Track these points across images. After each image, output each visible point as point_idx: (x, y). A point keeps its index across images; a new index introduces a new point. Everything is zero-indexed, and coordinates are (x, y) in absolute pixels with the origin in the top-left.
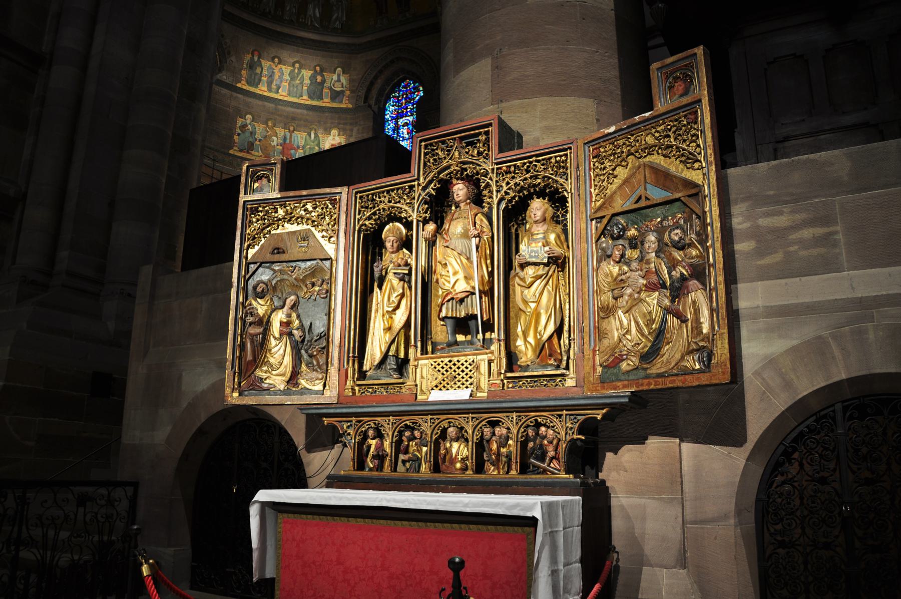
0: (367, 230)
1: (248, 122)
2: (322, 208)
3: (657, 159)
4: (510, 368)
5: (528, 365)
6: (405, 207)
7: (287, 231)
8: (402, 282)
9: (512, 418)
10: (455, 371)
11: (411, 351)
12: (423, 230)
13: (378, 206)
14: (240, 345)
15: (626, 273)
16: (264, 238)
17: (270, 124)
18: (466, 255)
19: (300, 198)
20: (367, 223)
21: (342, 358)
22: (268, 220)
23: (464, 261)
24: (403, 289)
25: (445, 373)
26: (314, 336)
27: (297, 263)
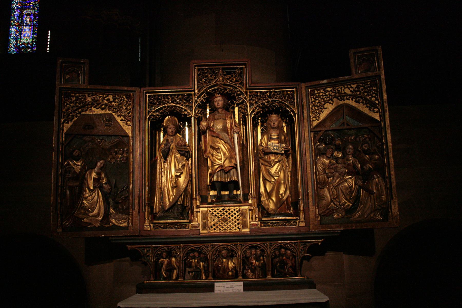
3: (352, 103)
7: (94, 113)
9: (267, 244)
15: (335, 164)
25: (220, 216)
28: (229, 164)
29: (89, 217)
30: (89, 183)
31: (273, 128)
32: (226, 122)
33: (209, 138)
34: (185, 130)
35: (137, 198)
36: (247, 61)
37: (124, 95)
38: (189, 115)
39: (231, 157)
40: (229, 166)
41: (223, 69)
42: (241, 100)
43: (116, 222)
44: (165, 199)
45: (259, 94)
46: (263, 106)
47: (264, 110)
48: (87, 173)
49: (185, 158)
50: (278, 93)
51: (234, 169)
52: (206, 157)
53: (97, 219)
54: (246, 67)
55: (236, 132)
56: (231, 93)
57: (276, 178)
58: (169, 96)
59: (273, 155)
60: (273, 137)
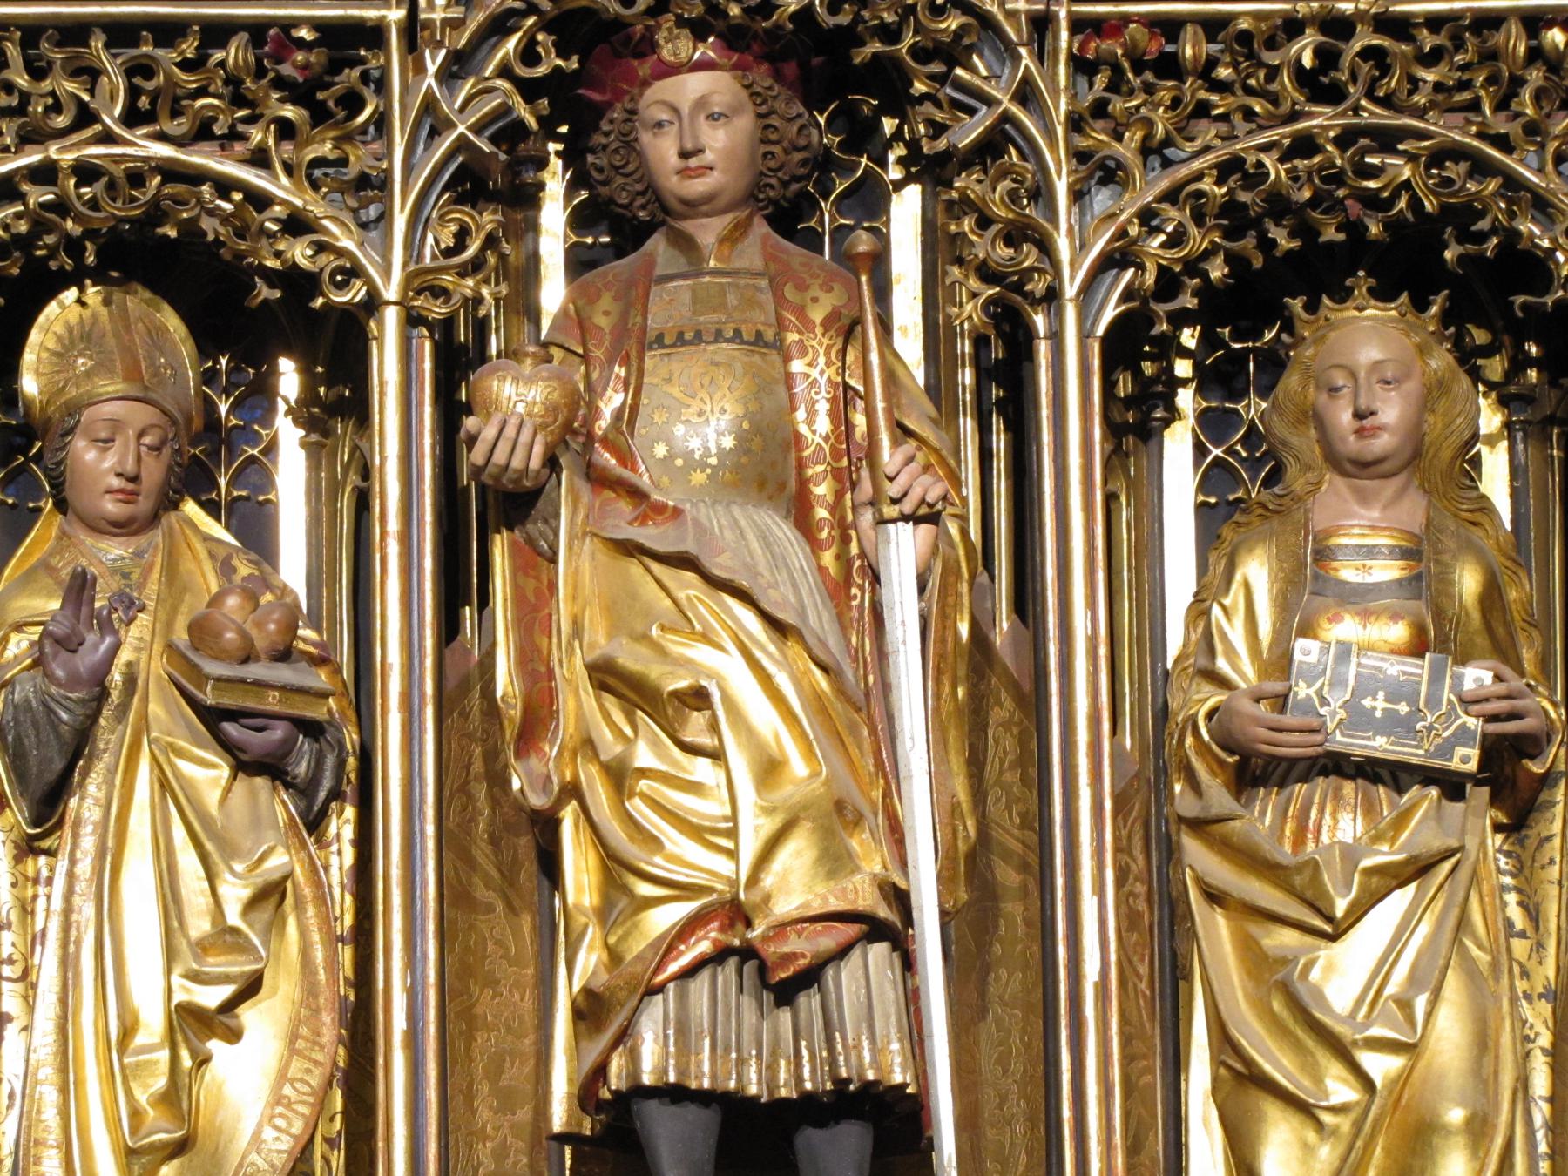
28: (821, 888)
31: (1361, 468)
32: (789, 378)
33: (575, 574)
34: (271, 449)
38: (342, 286)
39: (839, 806)
40: (817, 908)
42: (972, 112)
45: (1189, 52)
46: (1244, 197)
47: (1249, 242)
49: (281, 807)
51: (879, 951)
52: (537, 801)
55: (907, 507)
56: (857, 19)
57: (1380, 1066)
59: (1349, 788)
60: (1348, 573)
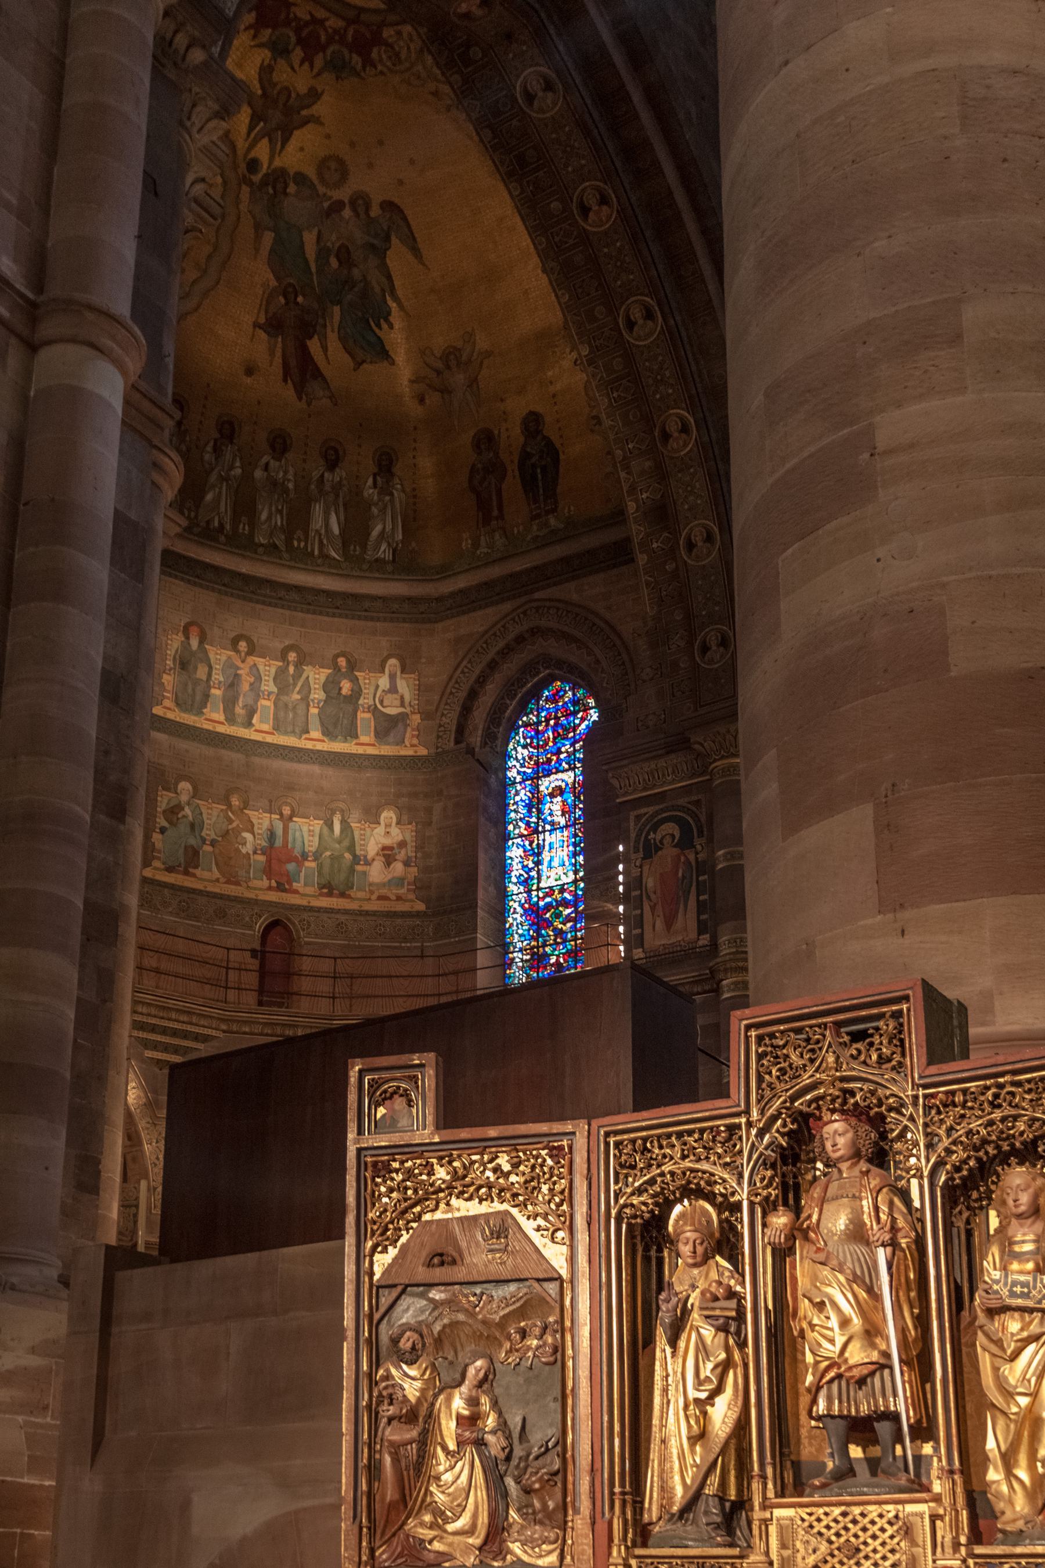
0: (635, 1217)
1: (184, 798)
2: (533, 1167)
4: (976, 1537)
5: (1021, 1531)
6: (719, 1172)
7: (457, 1215)
8: (722, 1335)
10: (856, 1536)
11: (756, 1485)
12: (764, 1225)
13: (659, 1166)
14: (369, 1467)
16: (408, 1230)
17: (235, 801)
18: (864, 1282)
19: (482, 1145)
20: (635, 1201)
21: (598, 1495)
22: (416, 1191)
23: (863, 1294)
24: (727, 1349)
26: (532, 1447)
27: (485, 1286)
28: (863, 1355)
29: (445, 1535)
30: (445, 1432)
35: (585, 1474)
36: (911, 988)
37: (543, 1149)
41: (838, 1025)
43: (525, 1552)
44: (672, 1478)
48: (439, 1401)
50: (1027, 1086)
53: (471, 1541)
54: (909, 1010)
55: (880, 1242)
58: (673, 1138)
